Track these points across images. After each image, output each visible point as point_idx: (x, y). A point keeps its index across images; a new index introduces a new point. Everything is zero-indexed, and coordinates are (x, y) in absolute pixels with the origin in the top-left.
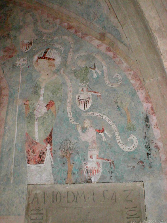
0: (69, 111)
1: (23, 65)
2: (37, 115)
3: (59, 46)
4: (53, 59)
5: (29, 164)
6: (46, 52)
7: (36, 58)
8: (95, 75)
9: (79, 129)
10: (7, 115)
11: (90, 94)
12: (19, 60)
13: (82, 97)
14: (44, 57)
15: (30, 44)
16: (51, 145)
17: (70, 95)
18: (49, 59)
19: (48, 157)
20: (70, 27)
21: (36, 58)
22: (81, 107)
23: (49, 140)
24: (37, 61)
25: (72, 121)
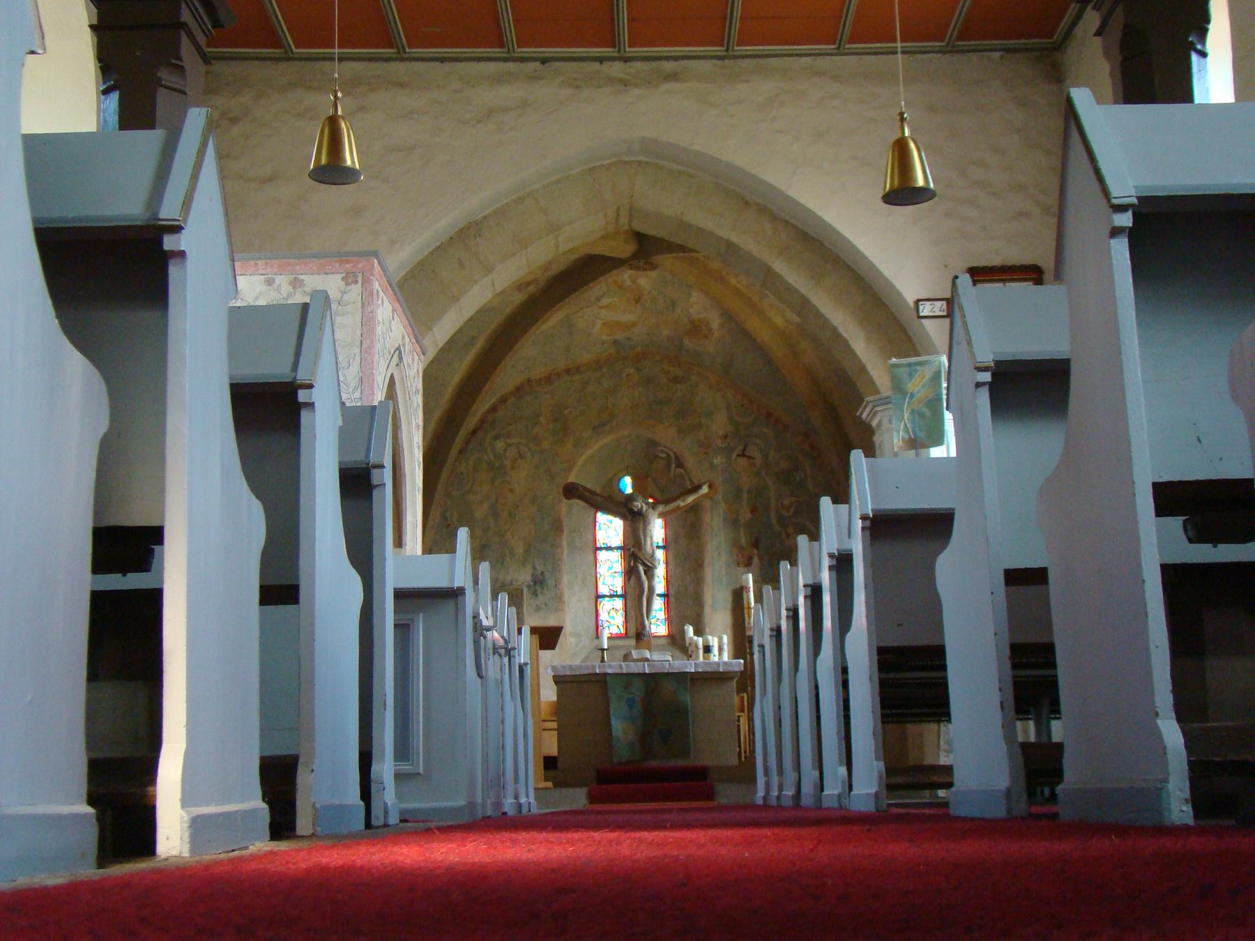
0: (773, 515)
1: (721, 464)
2: (742, 521)
3: (758, 441)
4: (754, 458)
5: (739, 566)
6: (745, 449)
7: (734, 456)
8: (798, 479)
9: (784, 534)
10: (712, 519)
11: (793, 499)
12: (717, 458)
13: (787, 502)
14: (743, 455)
15: (726, 437)
16: (758, 550)
17: (773, 502)
18: (749, 457)
19: (756, 560)
20: (769, 415)
21: (734, 456)
22: (785, 513)
23: (755, 545)
24: (736, 459)
25: (777, 528)
